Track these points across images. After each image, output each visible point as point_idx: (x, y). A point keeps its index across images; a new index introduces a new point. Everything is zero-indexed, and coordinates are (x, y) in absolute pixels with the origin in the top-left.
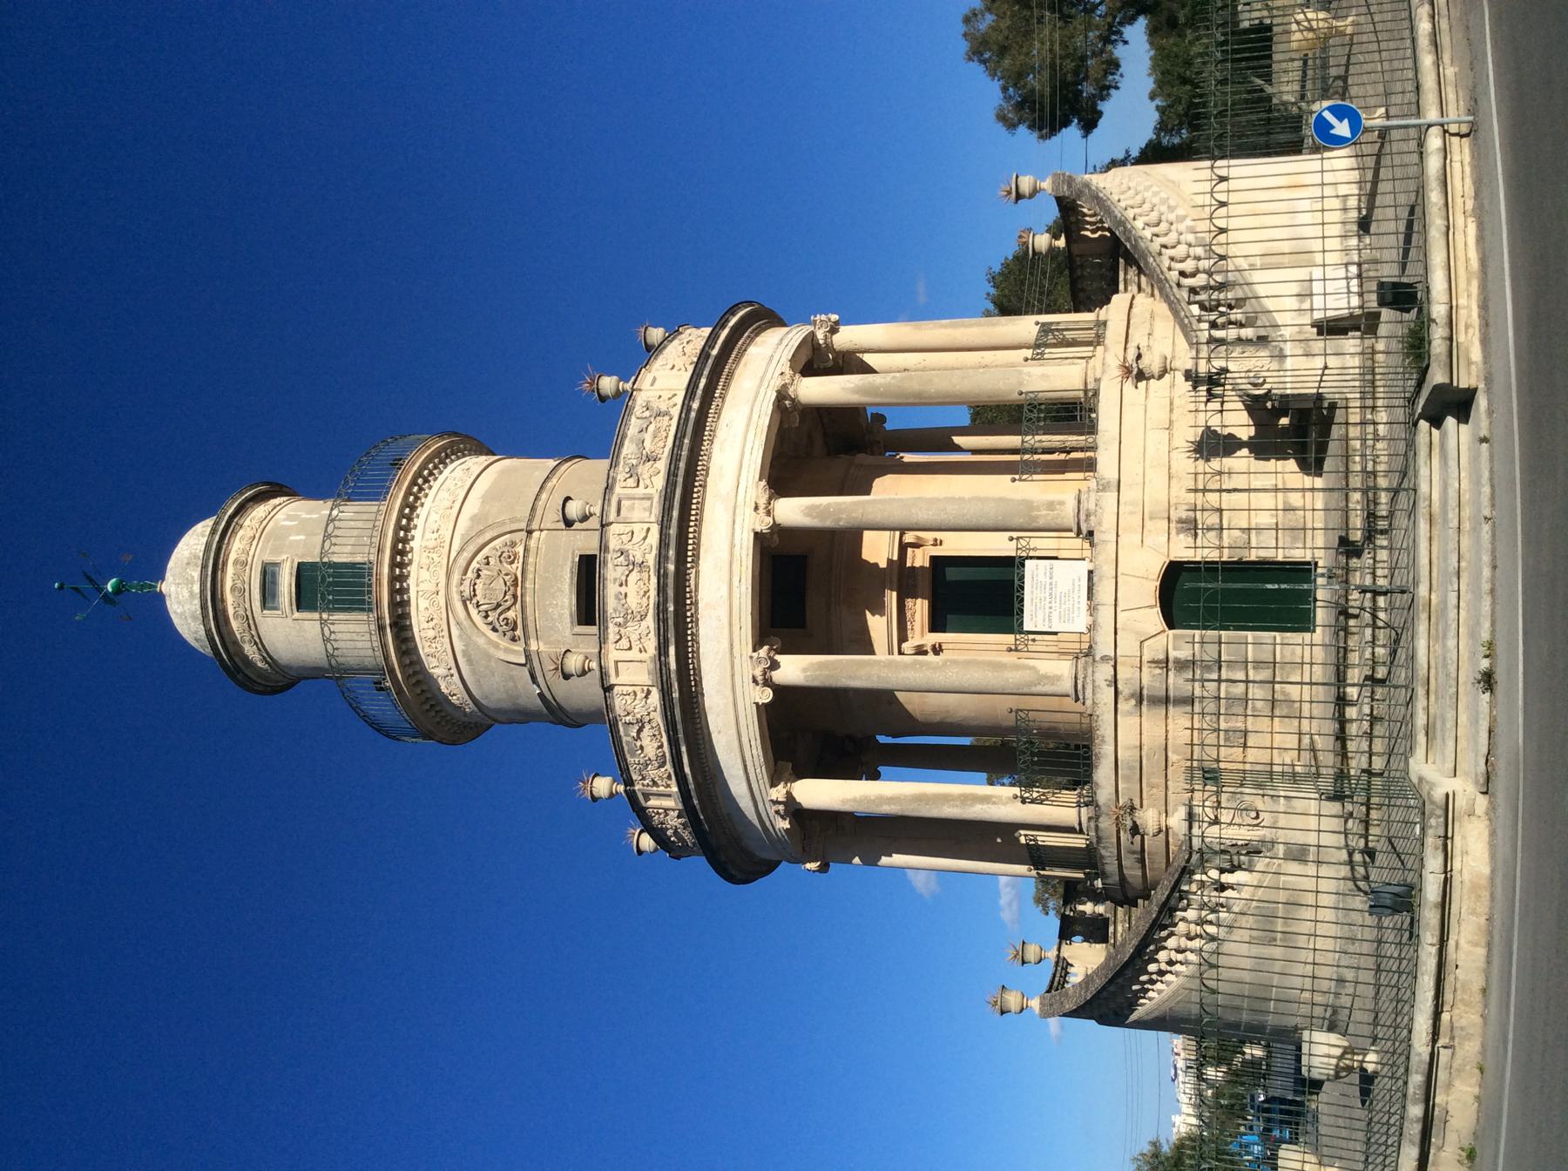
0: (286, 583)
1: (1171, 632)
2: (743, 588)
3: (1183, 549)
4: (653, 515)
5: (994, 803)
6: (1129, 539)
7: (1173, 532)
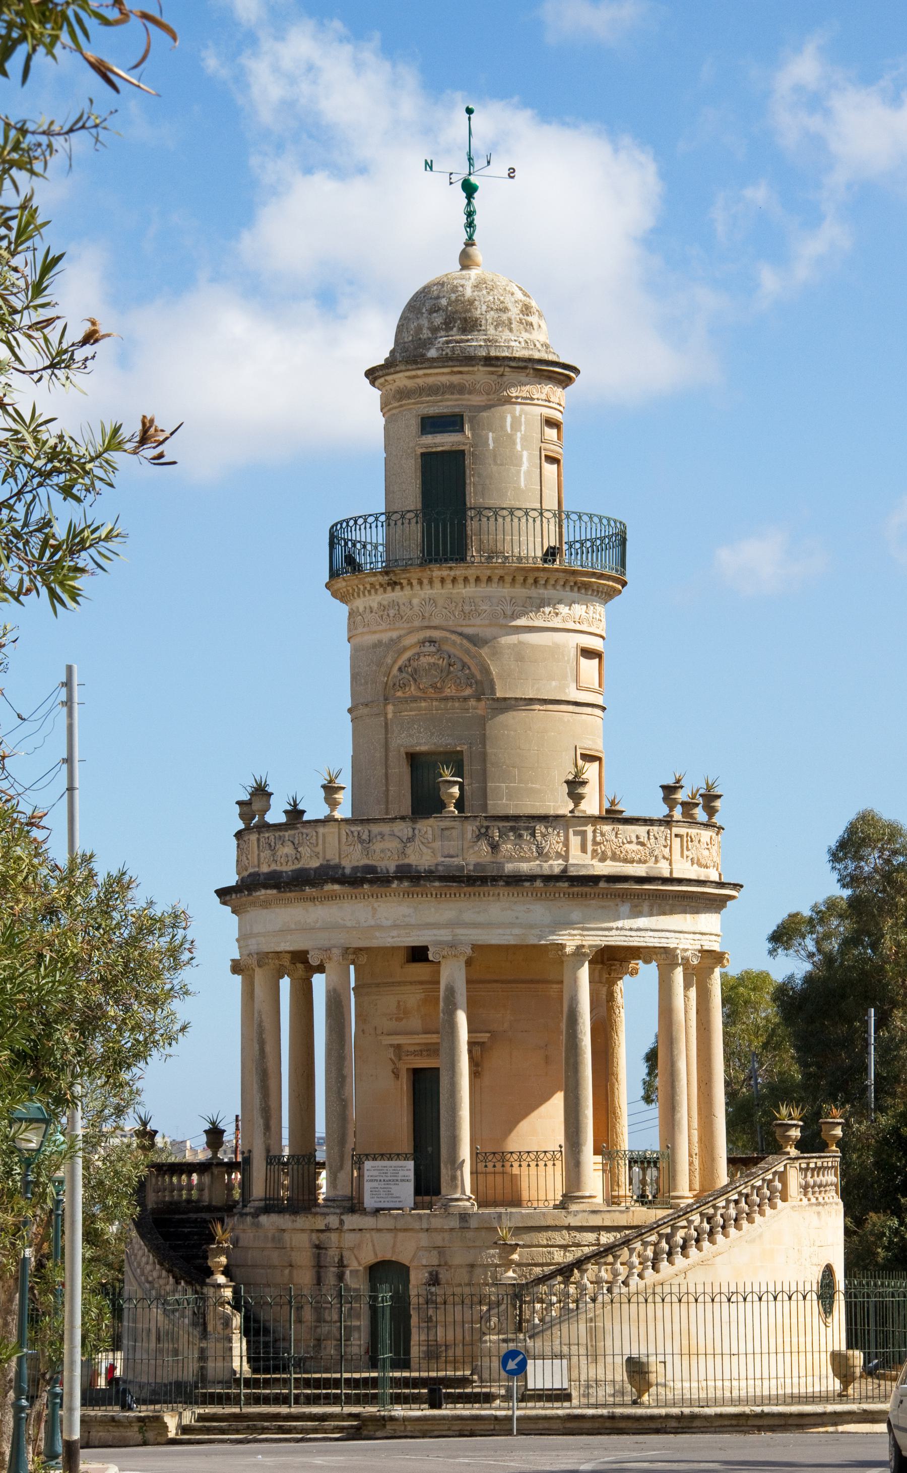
0: (444, 441)
1: (361, 1268)
2: (390, 940)
3: (417, 1278)
4: (443, 859)
5: (265, 1134)
6: (424, 1240)
7: (430, 1269)
